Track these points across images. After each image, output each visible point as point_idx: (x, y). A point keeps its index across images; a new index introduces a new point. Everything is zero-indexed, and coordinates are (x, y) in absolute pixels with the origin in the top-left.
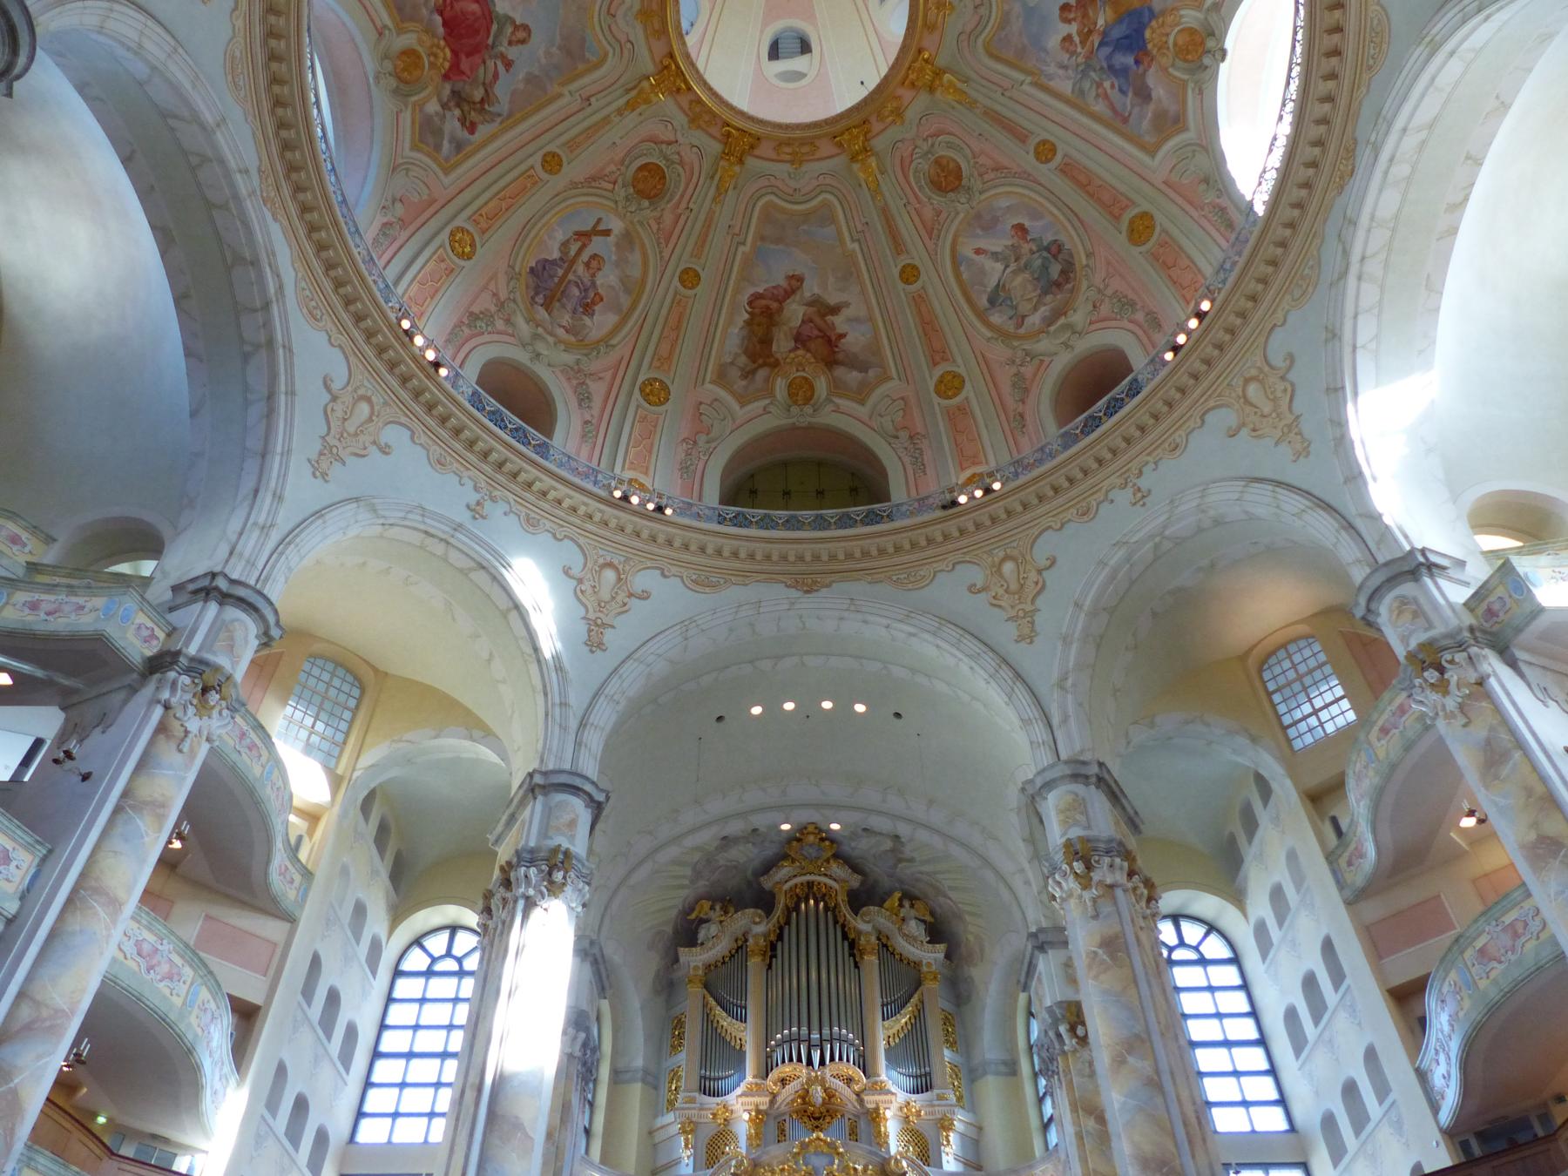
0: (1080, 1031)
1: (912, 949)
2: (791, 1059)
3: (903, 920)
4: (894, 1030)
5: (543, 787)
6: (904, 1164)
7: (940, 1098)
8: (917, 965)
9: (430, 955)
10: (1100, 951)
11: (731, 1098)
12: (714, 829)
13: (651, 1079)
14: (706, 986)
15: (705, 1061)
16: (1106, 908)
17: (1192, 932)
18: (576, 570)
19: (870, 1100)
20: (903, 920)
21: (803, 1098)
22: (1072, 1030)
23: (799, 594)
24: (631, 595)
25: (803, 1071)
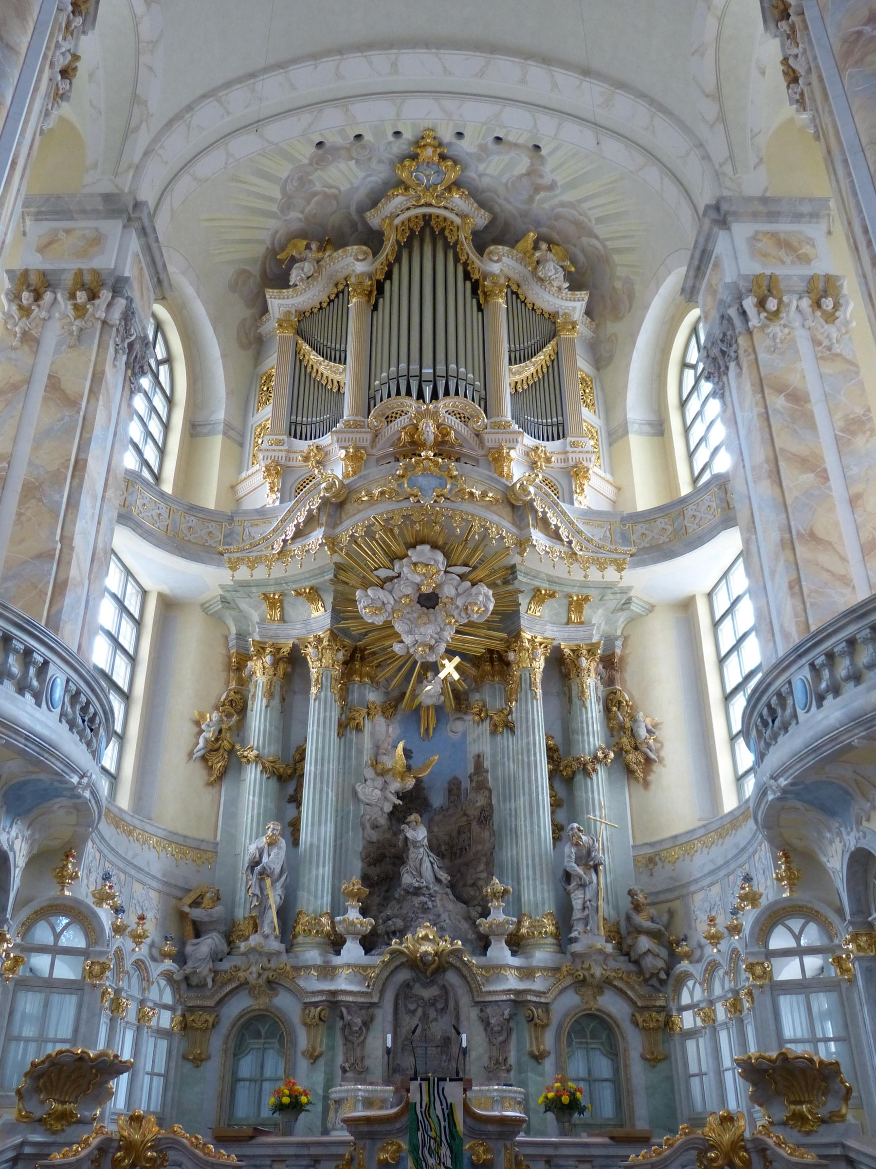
0: (772, 304)
1: (547, 297)
2: (398, 393)
3: (538, 262)
4: (523, 376)
6: (532, 489)
7: (574, 445)
8: (552, 318)
10: (868, 29)
11: (326, 440)
12: (306, 118)
13: (237, 436)
14: (299, 332)
15: (295, 406)
20: (538, 262)
21: (412, 436)
22: (761, 304)
25: (411, 405)
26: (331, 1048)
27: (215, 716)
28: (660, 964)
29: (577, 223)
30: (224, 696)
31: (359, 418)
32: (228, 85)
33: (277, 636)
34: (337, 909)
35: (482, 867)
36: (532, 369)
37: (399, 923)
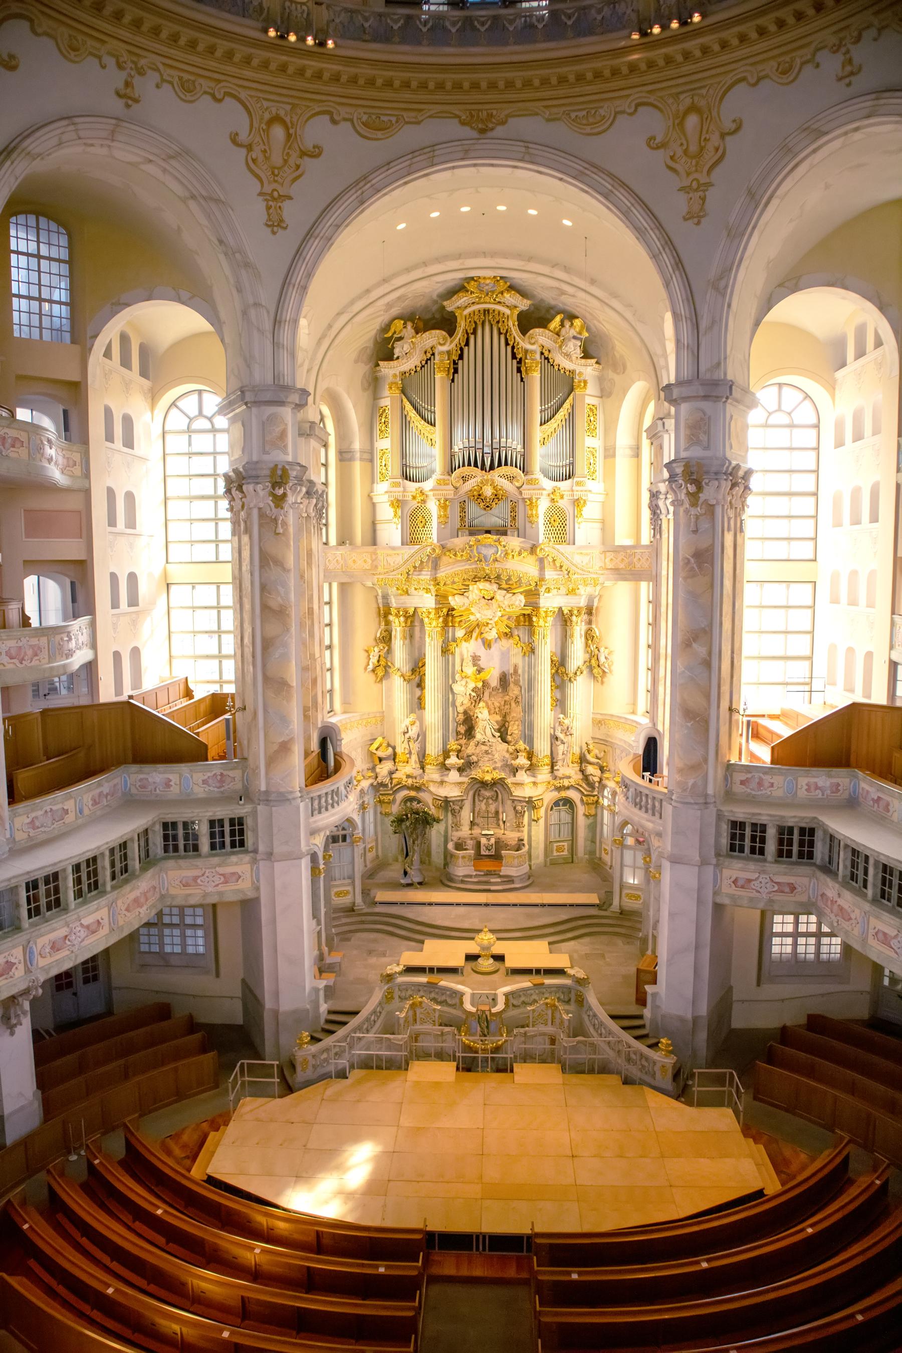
2: (469, 465)
5: (255, 402)
7: (578, 484)
8: (572, 372)
9: (188, 417)
10: (692, 560)
14: (403, 392)
16: (705, 525)
17: (791, 397)
18: (243, 137)
19: (526, 494)
23: (475, 134)
24: (303, 154)
26: (446, 816)
27: (376, 649)
28: (596, 779)
29: (591, 314)
30: (378, 635)
31: (447, 477)
32: (352, 302)
33: (405, 603)
34: (446, 754)
35: (516, 727)
36: (555, 425)
37: (474, 758)
